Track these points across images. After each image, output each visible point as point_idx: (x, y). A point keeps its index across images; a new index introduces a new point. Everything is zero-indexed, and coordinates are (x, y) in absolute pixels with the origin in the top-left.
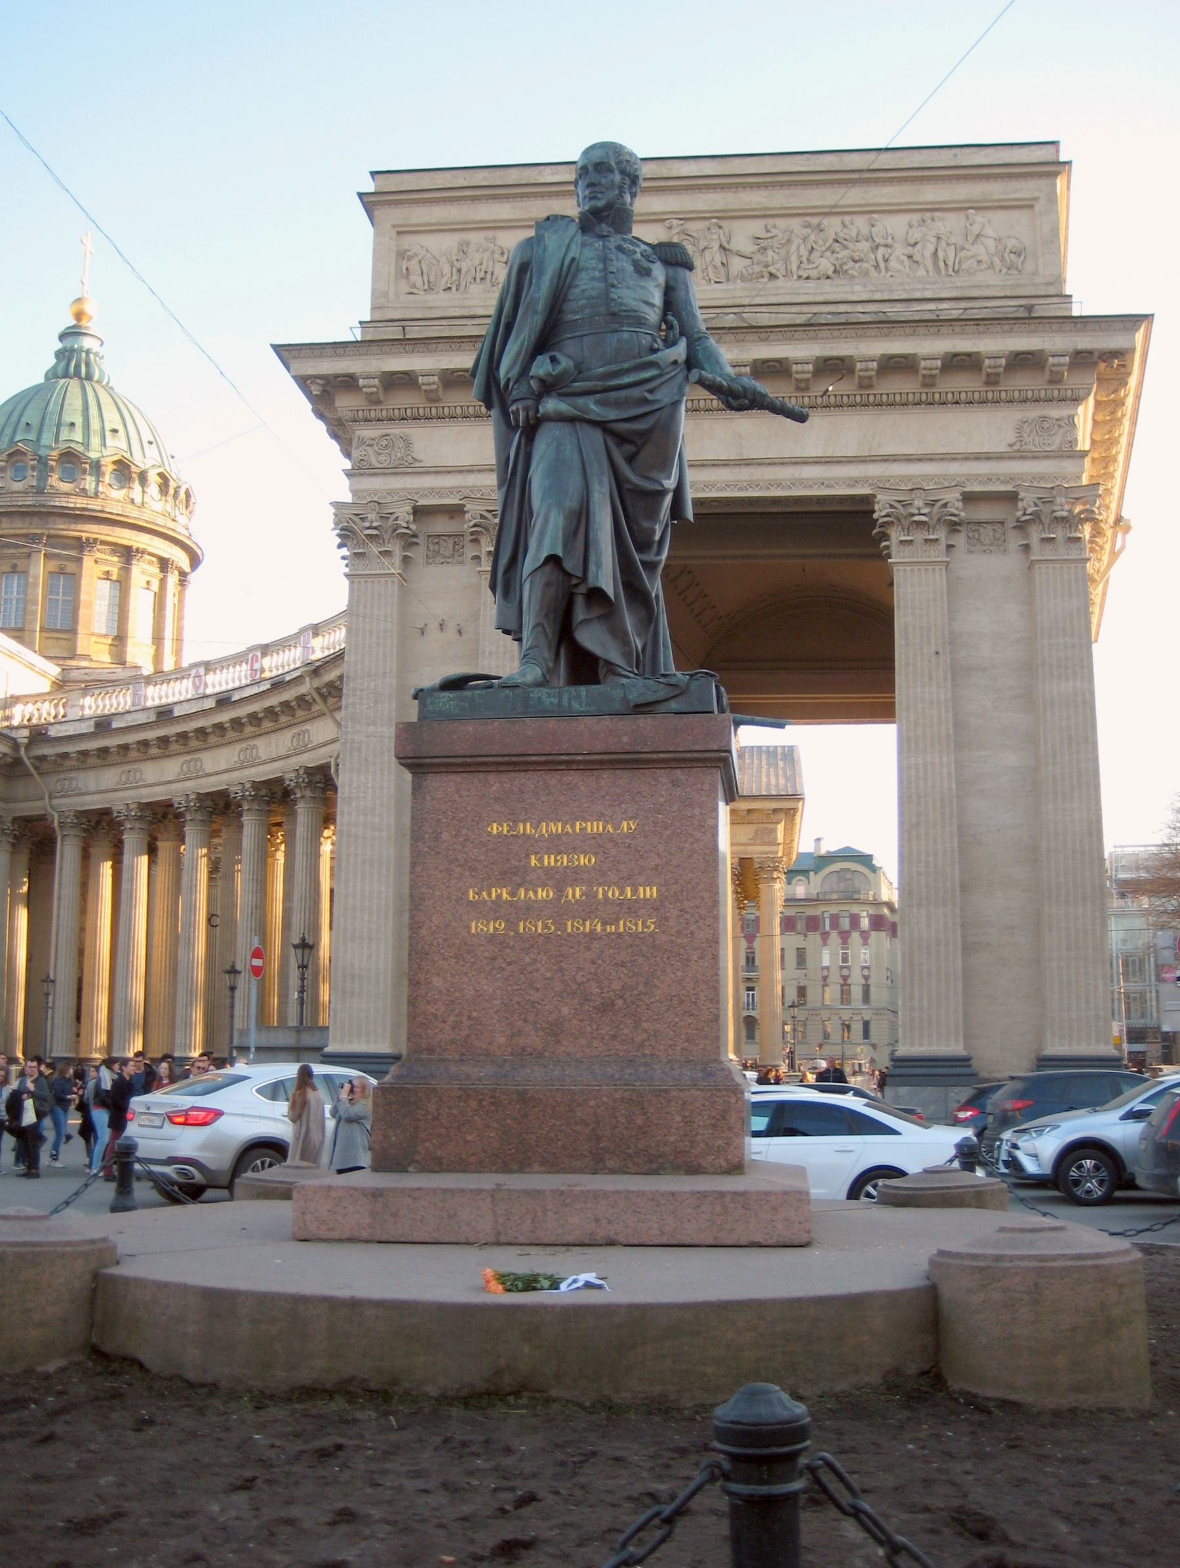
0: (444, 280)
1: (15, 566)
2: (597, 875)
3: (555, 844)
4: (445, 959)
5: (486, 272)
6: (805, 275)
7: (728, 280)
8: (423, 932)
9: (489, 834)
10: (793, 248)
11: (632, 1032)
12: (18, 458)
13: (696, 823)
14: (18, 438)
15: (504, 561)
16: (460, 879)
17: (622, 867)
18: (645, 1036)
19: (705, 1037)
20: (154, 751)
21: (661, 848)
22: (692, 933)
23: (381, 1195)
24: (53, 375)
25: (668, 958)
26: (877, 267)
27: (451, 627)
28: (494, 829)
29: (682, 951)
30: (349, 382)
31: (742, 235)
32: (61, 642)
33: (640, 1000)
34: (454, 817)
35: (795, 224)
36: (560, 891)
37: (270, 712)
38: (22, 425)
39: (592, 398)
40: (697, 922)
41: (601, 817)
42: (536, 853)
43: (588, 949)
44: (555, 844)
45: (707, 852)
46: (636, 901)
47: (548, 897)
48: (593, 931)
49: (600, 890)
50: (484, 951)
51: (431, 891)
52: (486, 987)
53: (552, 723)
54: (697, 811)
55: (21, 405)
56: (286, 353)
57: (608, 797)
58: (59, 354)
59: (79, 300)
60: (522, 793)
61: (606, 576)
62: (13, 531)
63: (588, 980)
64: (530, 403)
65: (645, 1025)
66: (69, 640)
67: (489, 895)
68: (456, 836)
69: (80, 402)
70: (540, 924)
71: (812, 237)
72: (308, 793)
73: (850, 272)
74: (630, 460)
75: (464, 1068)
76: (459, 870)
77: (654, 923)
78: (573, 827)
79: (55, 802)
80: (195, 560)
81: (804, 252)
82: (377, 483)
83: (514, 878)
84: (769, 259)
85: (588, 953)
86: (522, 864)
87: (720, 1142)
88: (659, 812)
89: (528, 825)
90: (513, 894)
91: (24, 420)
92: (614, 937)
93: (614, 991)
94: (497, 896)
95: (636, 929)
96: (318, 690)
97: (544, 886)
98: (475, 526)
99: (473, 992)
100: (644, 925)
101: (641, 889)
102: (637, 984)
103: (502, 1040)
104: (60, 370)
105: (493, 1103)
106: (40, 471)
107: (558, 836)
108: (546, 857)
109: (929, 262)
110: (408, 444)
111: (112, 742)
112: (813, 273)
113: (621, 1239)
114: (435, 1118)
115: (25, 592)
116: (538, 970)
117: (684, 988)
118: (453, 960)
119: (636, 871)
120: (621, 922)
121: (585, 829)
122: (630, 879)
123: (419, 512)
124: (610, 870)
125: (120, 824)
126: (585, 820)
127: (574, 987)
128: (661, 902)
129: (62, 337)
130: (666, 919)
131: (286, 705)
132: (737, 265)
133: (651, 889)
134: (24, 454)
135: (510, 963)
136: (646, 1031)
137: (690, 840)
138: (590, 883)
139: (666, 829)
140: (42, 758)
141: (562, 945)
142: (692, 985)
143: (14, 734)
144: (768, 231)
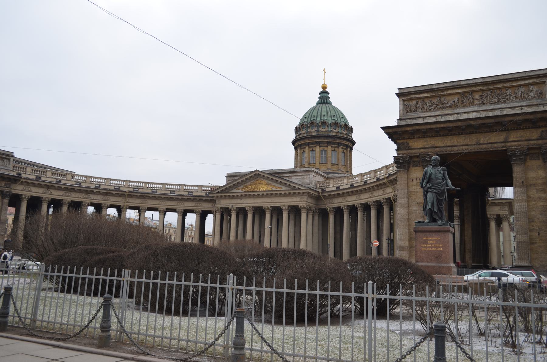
1: (313, 149)
2: (436, 243)
10: (488, 97)
14: (312, 119)
15: (424, 207)
20: (350, 194)
24: (318, 103)
26: (508, 100)
27: (418, 179)
28: (424, 238)
30: (395, 133)
31: (477, 96)
32: (324, 166)
35: (489, 92)
36: (431, 245)
37: (377, 186)
38: (313, 116)
44: (431, 240)
55: (312, 110)
56: (383, 128)
58: (319, 98)
61: (436, 210)
71: (493, 94)
72: (386, 204)
74: (439, 196)
79: (328, 205)
80: (354, 143)
81: (491, 98)
82: (402, 152)
84: (483, 100)
96: (388, 181)
104: (320, 102)
109: (520, 98)
110: (408, 144)
111: (340, 192)
112: (493, 102)
115: (315, 155)
122: (439, 244)
123: (411, 157)
125: (343, 210)
129: (320, 94)
131: (380, 184)
132: (476, 102)
134: (314, 123)
140: (325, 196)
143: (318, 190)
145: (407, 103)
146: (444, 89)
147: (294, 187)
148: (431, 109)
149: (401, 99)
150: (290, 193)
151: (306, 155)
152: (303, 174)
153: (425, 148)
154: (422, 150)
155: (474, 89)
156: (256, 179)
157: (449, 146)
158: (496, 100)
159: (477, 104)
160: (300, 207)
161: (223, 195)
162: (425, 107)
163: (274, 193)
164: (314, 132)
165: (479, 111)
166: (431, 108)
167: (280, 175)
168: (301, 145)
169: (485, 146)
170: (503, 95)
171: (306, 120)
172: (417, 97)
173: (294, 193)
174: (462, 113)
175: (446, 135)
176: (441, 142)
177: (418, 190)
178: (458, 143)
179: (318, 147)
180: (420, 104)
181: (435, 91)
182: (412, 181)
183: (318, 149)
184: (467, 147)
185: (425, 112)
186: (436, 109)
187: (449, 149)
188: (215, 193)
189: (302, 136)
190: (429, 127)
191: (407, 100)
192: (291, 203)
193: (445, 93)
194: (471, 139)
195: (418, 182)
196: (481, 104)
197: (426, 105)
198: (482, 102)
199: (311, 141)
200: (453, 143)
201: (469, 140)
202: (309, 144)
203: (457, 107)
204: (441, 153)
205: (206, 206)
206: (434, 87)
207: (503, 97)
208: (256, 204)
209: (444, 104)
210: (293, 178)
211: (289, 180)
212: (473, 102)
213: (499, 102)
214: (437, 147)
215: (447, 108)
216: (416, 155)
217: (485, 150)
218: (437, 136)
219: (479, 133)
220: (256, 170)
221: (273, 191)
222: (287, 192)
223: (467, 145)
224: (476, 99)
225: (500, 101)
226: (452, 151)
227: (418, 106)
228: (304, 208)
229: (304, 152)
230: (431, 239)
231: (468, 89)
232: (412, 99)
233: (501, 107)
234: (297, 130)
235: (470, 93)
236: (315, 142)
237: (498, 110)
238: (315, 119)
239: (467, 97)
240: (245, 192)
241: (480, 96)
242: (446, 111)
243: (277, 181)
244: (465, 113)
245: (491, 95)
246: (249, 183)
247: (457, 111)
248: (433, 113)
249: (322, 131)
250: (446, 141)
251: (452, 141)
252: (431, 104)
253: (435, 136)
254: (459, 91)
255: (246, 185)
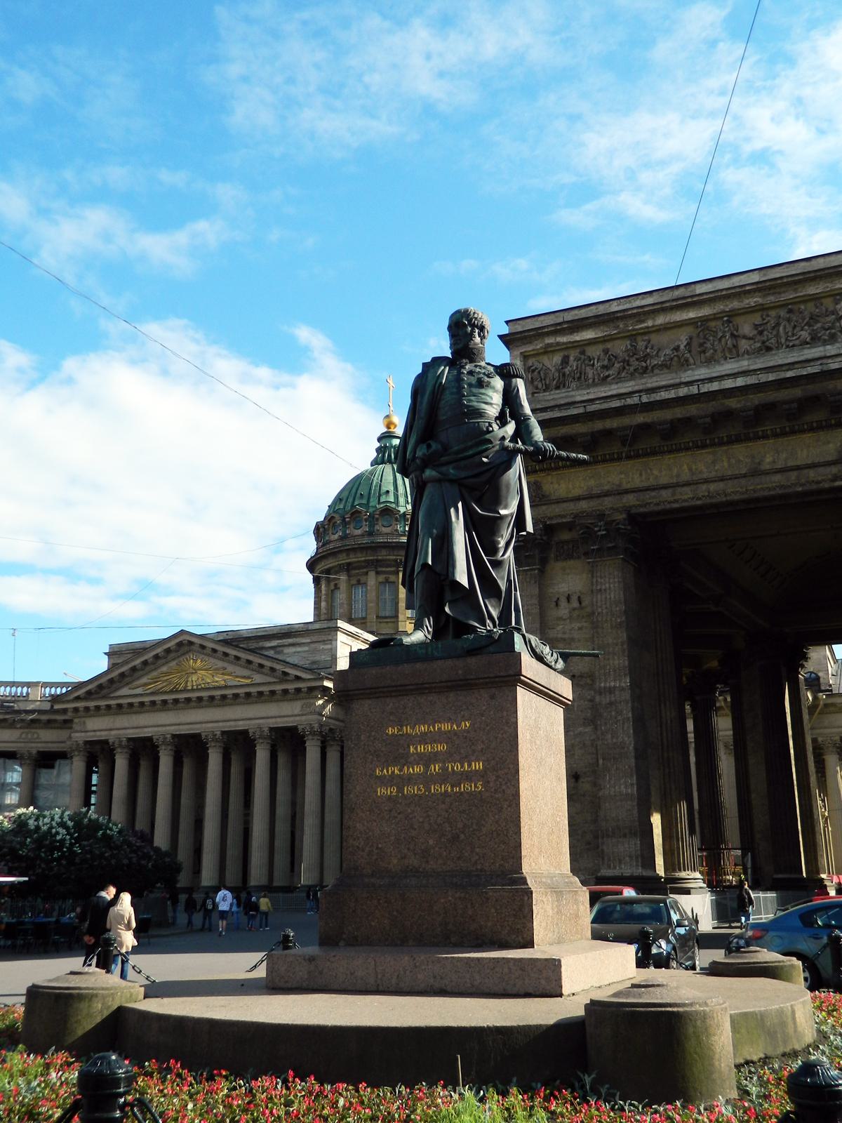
0: (555, 382)
2: (449, 756)
3: (424, 739)
4: (363, 812)
5: (581, 374)
6: (791, 344)
7: (738, 356)
8: (352, 796)
9: (387, 734)
11: (469, 855)
12: (357, 515)
13: (504, 721)
16: (371, 763)
17: (462, 751)
18: (477, 857)
19: (513, 858)
21: (484, 738)
22: (503, 790)
23: (314, 960)
24: (375, 462)
25: (490, 807)
28: (390, 731)
29: (498, 802)
32: (390, 625)
33: (474, 834)
34: (368, 726)
35: (783, 313)
36: (427, 767)
38: (358, 495)
39: (451, 466)
40: (506, 783)
41: (449, 720)
42: (413, 745)
43: (444, 803)
44: (424, 739)
45: (511, 739)
46: (471, 771)
47: (420, 771)
48: (446, 791)
49: (450, 765)
50: (385, 806)
51: (355, 771)
52: (386, 829)
53: (418, 666)
54: (505, 713)
57: (453, 708)
58: (378, 450)
59: (388, 416)
60: (405, 708)
62: (356, 560)
63: (444, 823)
64: (418, 473)
65: (477, 850)
66: (394, 622)
67: (388, 772)
68: (369, 737)
69: (392, 478)
70: (416, 788)
73: (823, 337)
75: (372, 880)
76: (371, 757)
77: (481, 785)
78: (434, 728)
81: (789, 329)
83: (401, 761)
84: (765, 338)
85: (443, 805)
86: (406, 751)
87: (519, 926)
88: (482, 715)
89: (409, 727)
90: (400, 770)
91: (359, 492)
92: (458, 794)
93: (459, 829)
94: (391, 772)
95: (471, 789)
97: (418, 764)
98: (582, 533)
99: (379, 832)
100: (475, 786)
101: (473, 763)
102: (472, 823)
103: (395, 861)
105: (386, 902)
106: (370, 522)
107: (425, 734)
108: (419, 747)
112: (797, 342)
113: (449, 989)
114: (354, 911)
116: (415, 817)
117: (500, 826)
118: (368, 813)
119: (470, 753)
120: (462, 786)
121: (441, 728)
122: (466, 758)
124: (455, 753)
126: (440, 722)
127: (436, 827)
128: (485, 772)
129: (379, 440)
130: (488, 782)
132: (744, 345)
133: (479, 764)
135: (399, 813)
136: (477, 854)
137: (502, 732)
138: (444, 762)
139: (487, 726)
141: (429, 801)
142: (504, 824)
144: (764, 319)
145: (537, 364)
146: (645, 313)
147: (285, 674)
148: (608, 376)
149: (517, 353)
150: (273, 693)
151: (341, 596)
152: (315, 638)
153: (590, 497)
154: (584, 505)
155: (735, 304)
156: (184, 657)
157: (665, 487)
158: (805, 335)
159: (748, 352)
160: (300, 730)
161: (92, 704)
162: (590, 373)
163: (229, 692)
164: (362, 535)
165: (755, 370)
166: (607, 374)
167: (253, 645)
168: (328, 571)
169: (777, 478)
170: (828, 319)
171: (342, 506)
172: (564, 344)
173: (285, 692)
174: (703, 380)
175: (653, 453)
176: (641, 475)
177: (576, 635)
178: (693, 474)
179: (372, 574)
180: (575, 364)
181: (617, 318)
182: (557, 605)
183: (372, 580)
184: (721, 486)
185: (588, 387)
186: (623, 375)
187: (665, 494)
188: (68, 702)
189: (331, 546)
190: (599, 425)
191: (534, 356)
192: (279, 720)
193: (650, 323)
194: (733, 461)
195: (574, 609)
196: (760, 349)
197: (593, 365)
198: (764, 342)
199: (353, 559)
200: (678, 476)
201: (726, 464)
202: (348, 568)
203: (684, 364)
204: (642, 510)
205: (48, 739)
206: (615, 308)
207: (826, 326)
208: (181, 727)
209: (646, 357)
210: (286, 650)
211: (277, 656)
212: (734, 346)
213: (815, 340)
214: (627, 492)
215: (656, 371)
216: (564, 520)
217: (780, 492)
218: (629, 457)
219: (757, 438)
220: (182, 632)
221: (226, 687)
222: (265, 689)
223: (722, 479)
224: (745, 337)
225: (819, 338)
226: (676, 501)
227: (567, 370)
228: (313, 733)
229: (336, 587)
230: (424, 734)
231: (720, 307)
232: (547, 351)
233: (822, 354)
234: (320, 531)
235: (725, 319)
236: (365, 561)
237: (812, 364)
238: (364, 501)
239: (716, 332)
240: (152, 694)
241: (756, 326)
242: (655, 379)
243: (237, 658)
244: (711, 380)
245: (789, 320)
246: (164, 669)
247: (687, 376)
248: (614, 386)
249: (381, 534)
250: (656, 472)
251: (675, 471)
252: (606, 362)
253: (619, 459)
254: (692, 314)
255: (155, 674)
